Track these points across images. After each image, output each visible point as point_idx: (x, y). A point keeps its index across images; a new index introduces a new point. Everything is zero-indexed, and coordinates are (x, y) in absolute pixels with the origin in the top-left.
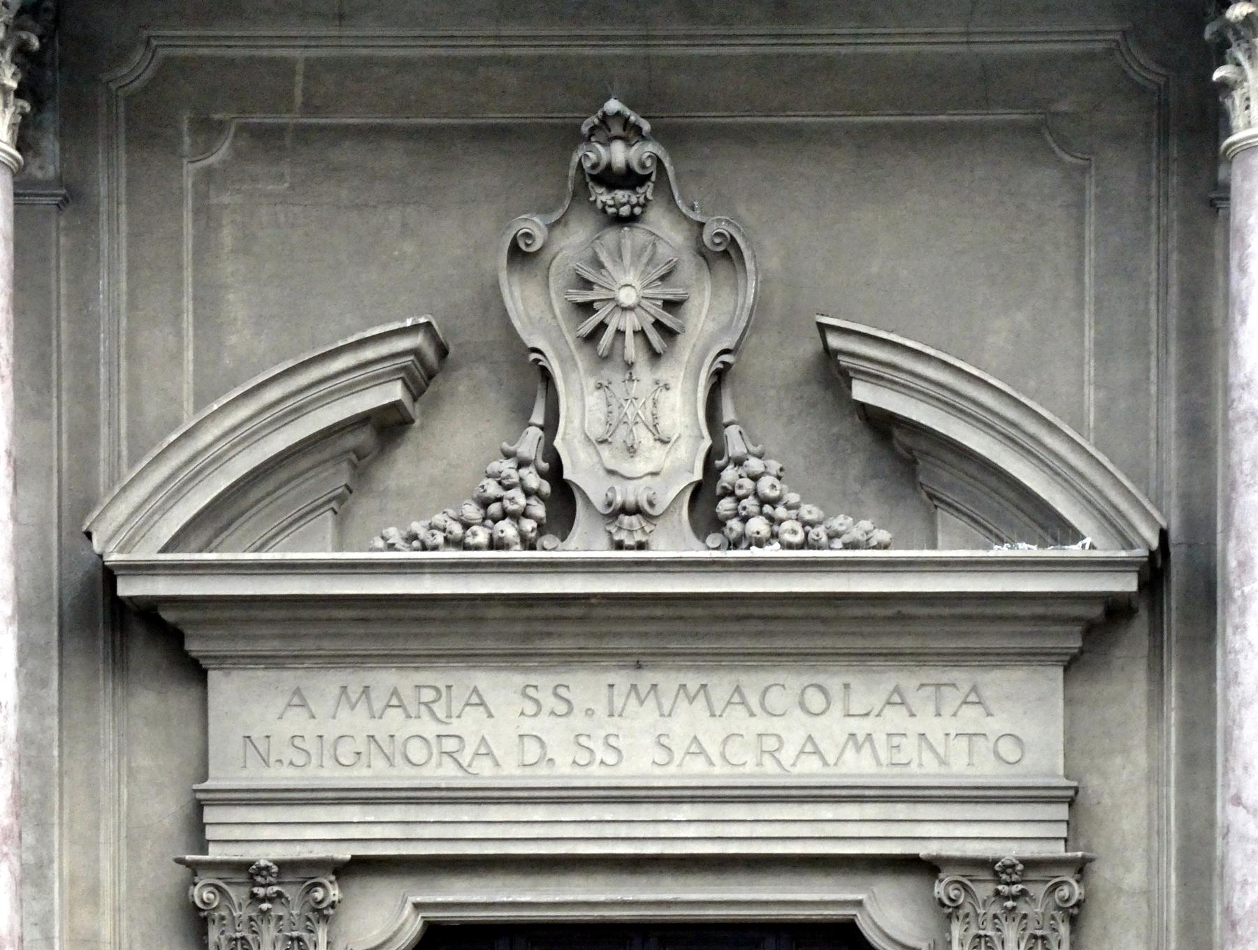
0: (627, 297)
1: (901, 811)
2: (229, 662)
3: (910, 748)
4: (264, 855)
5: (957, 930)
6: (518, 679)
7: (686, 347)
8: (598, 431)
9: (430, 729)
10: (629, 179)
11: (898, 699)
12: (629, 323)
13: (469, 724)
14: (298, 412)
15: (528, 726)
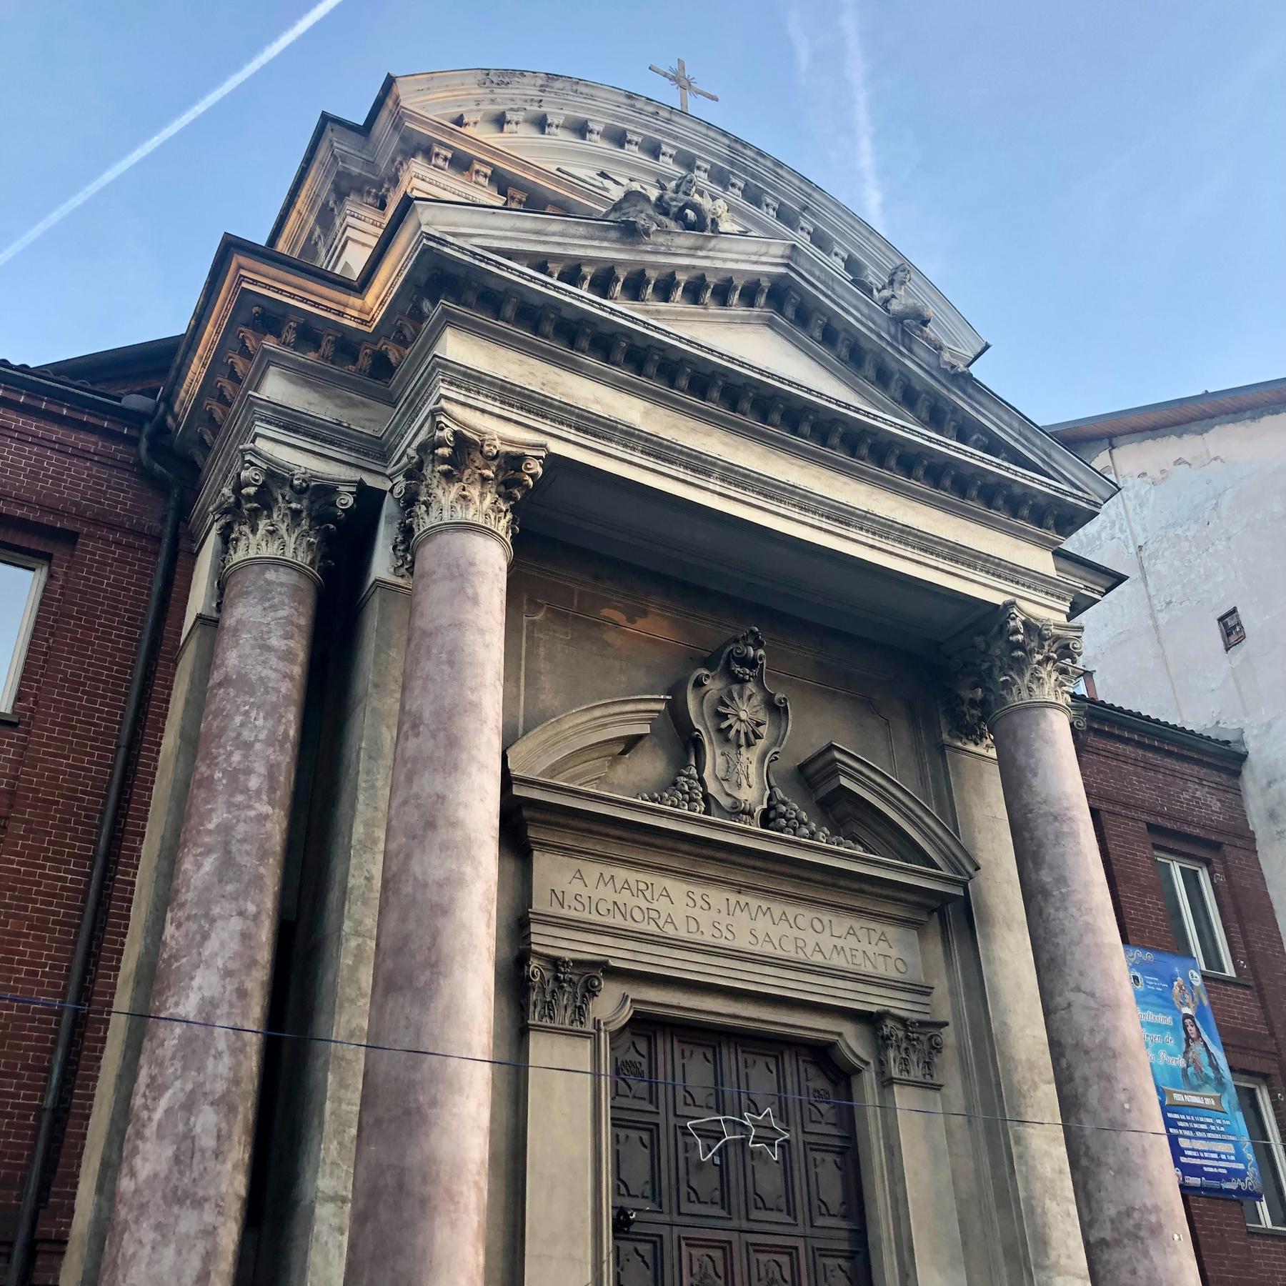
0: (743, 716)
1: (861, 987)
2: (546, 846)
3: (859, 959)
4: (568, 955)
5: (891, 1054)
6: (685, 887)
7: (761, 744)
8: (721, 774)
9: (644, 905)
10: (752, 663)
11: (851, 932)
12: (743, 728)
13: (662, 904)
14: (604, 726)
15: (690, 912)
